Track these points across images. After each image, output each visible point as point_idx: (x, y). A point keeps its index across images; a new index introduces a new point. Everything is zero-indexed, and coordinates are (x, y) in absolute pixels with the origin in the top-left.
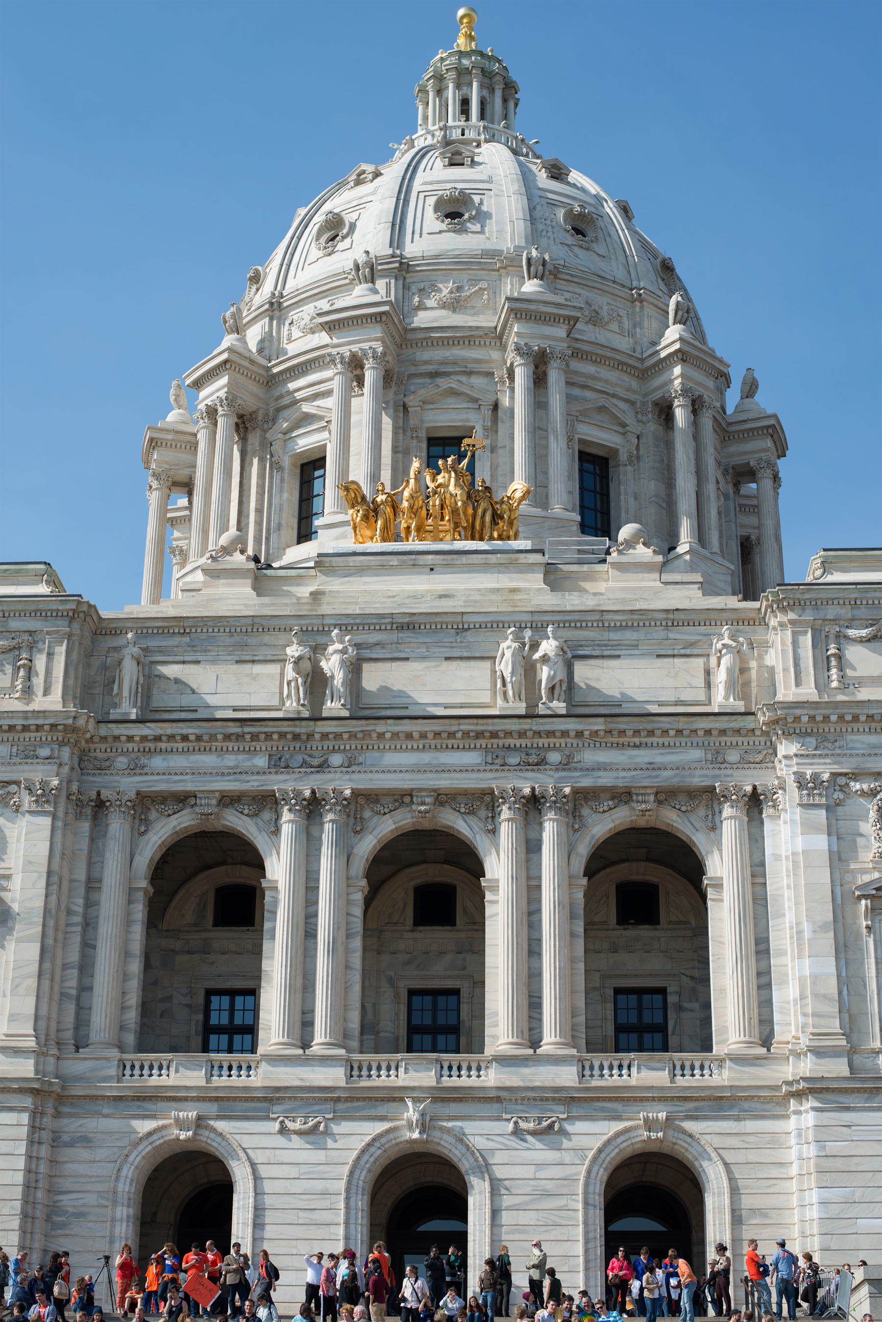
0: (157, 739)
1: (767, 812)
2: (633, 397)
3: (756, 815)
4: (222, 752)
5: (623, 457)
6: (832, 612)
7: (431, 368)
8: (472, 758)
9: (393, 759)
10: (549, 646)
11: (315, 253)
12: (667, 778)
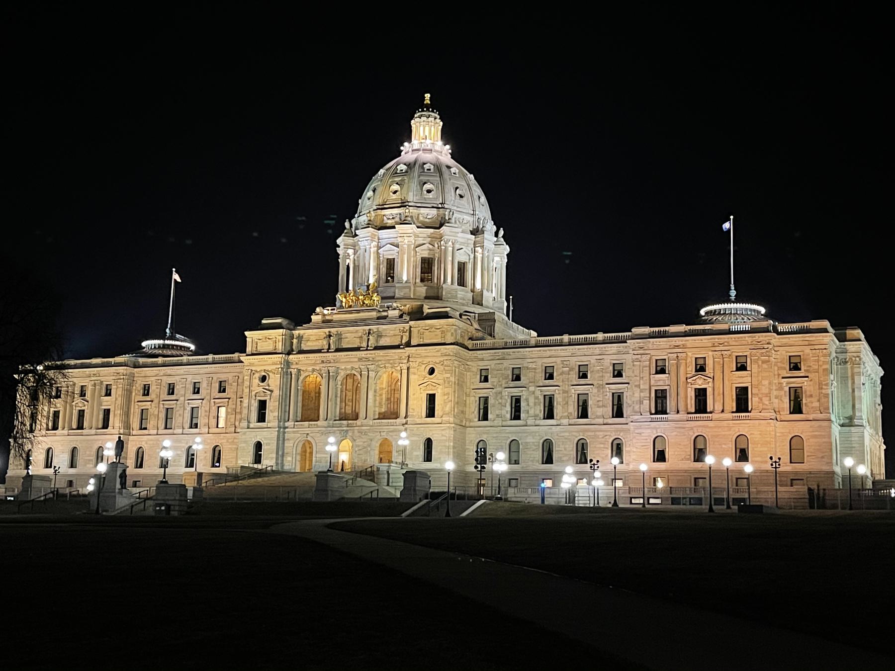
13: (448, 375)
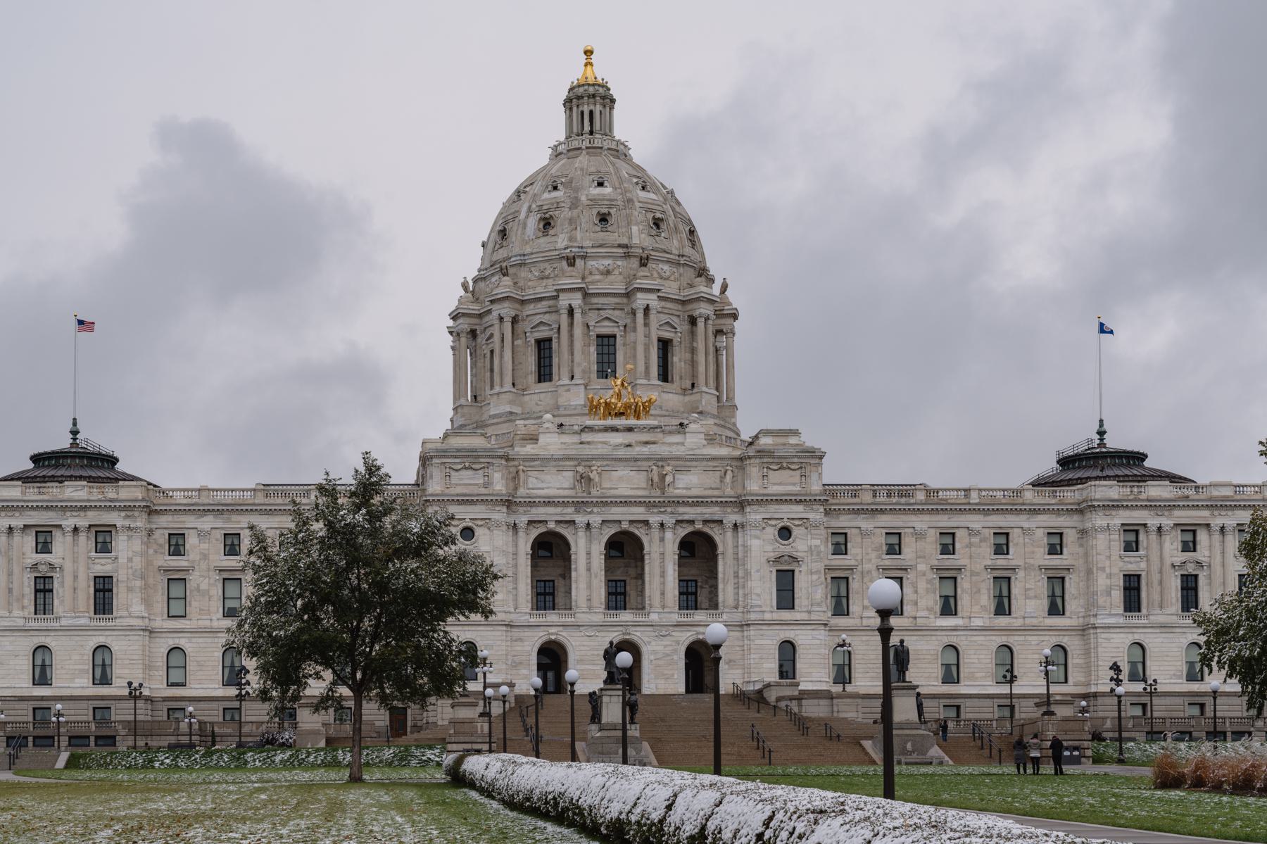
1: (739, 530)
2: (678, 313)
3: (735, 535)
5: (675, 343)
6: (765, 460)
8: (641, 510)
9: (615, 510)
10: (668, 469)
11: (541, 234)
12: (707, 517)
13: (818, 542)
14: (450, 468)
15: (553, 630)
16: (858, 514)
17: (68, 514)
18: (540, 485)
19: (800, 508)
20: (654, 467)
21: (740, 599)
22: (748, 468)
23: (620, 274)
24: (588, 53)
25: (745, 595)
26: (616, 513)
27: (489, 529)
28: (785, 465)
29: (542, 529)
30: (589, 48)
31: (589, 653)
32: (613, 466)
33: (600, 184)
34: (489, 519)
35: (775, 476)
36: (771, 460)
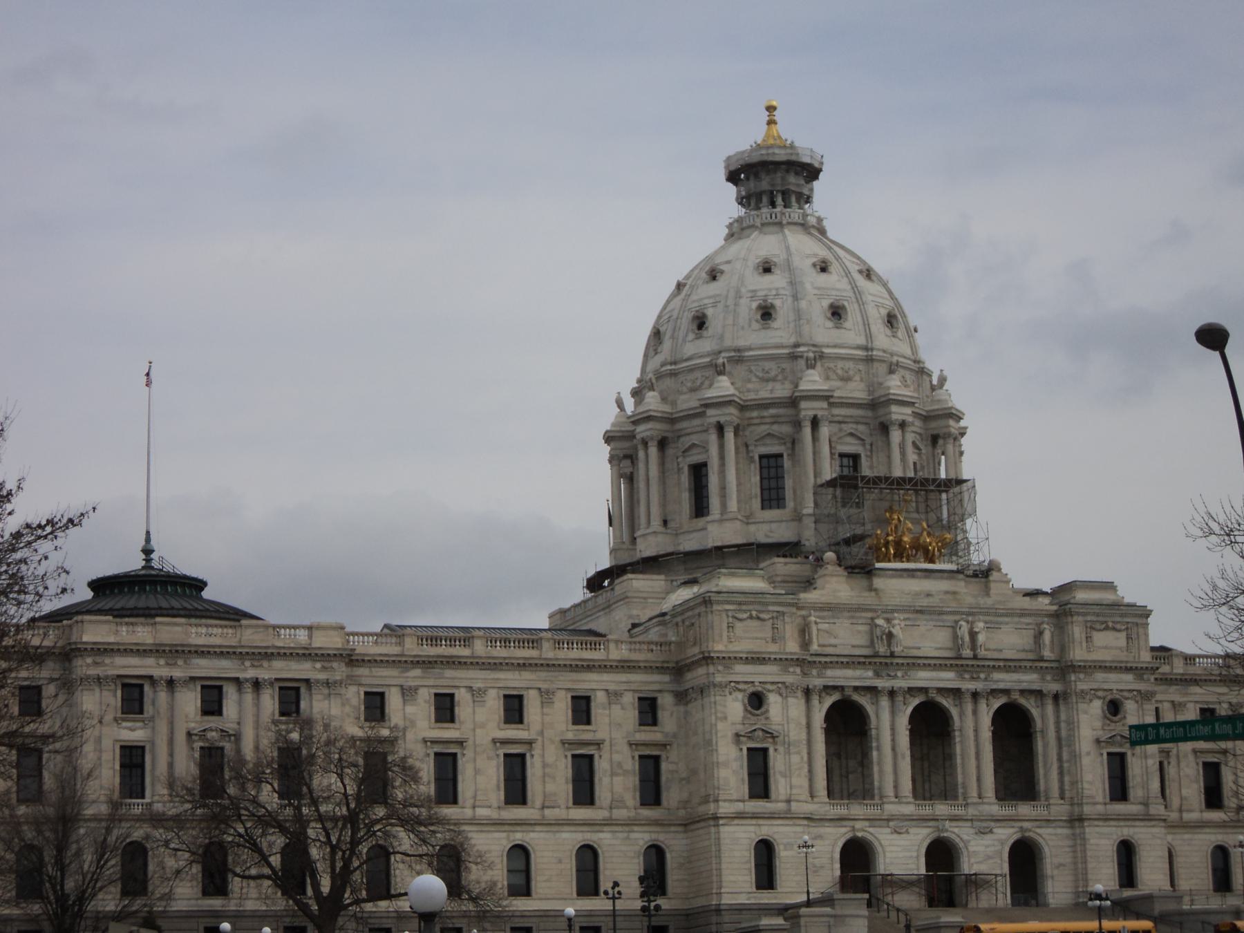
0: (831, 662)
1: (1061, 702)
4: (855, 669)
6: (1089, 618)
7: (840, 419)
8: (950, 675)
11: (756, 326)
12: (1024, 686)
14: (734, 617)
15: (858, 825)
16: (1171, 685)
17: (248, 663)
18: (833, 641)
19: (1129, 677)
20: (963, 623)
21: (1067, 787)
22: (1070, 627)
23: (862, 380)
24: (771, 109)
25: (1074, 783)
26: (923, 678)
27: (781, 695)
28: (1110, 624)
29: (836, 697)
30: (774, 103)
31: (901, 855)
32: (915, 619)
33: (823, 270)
34: (783, 683)
35: (1101, 638)
36: (1094, 618)
